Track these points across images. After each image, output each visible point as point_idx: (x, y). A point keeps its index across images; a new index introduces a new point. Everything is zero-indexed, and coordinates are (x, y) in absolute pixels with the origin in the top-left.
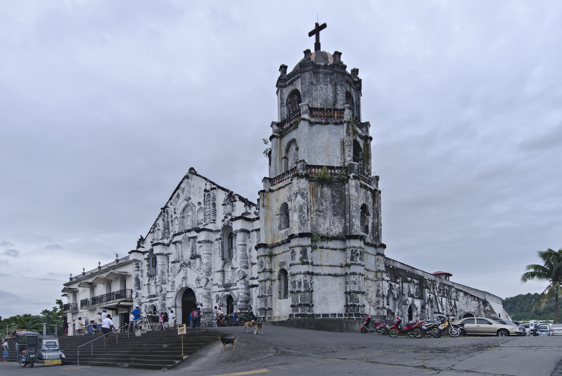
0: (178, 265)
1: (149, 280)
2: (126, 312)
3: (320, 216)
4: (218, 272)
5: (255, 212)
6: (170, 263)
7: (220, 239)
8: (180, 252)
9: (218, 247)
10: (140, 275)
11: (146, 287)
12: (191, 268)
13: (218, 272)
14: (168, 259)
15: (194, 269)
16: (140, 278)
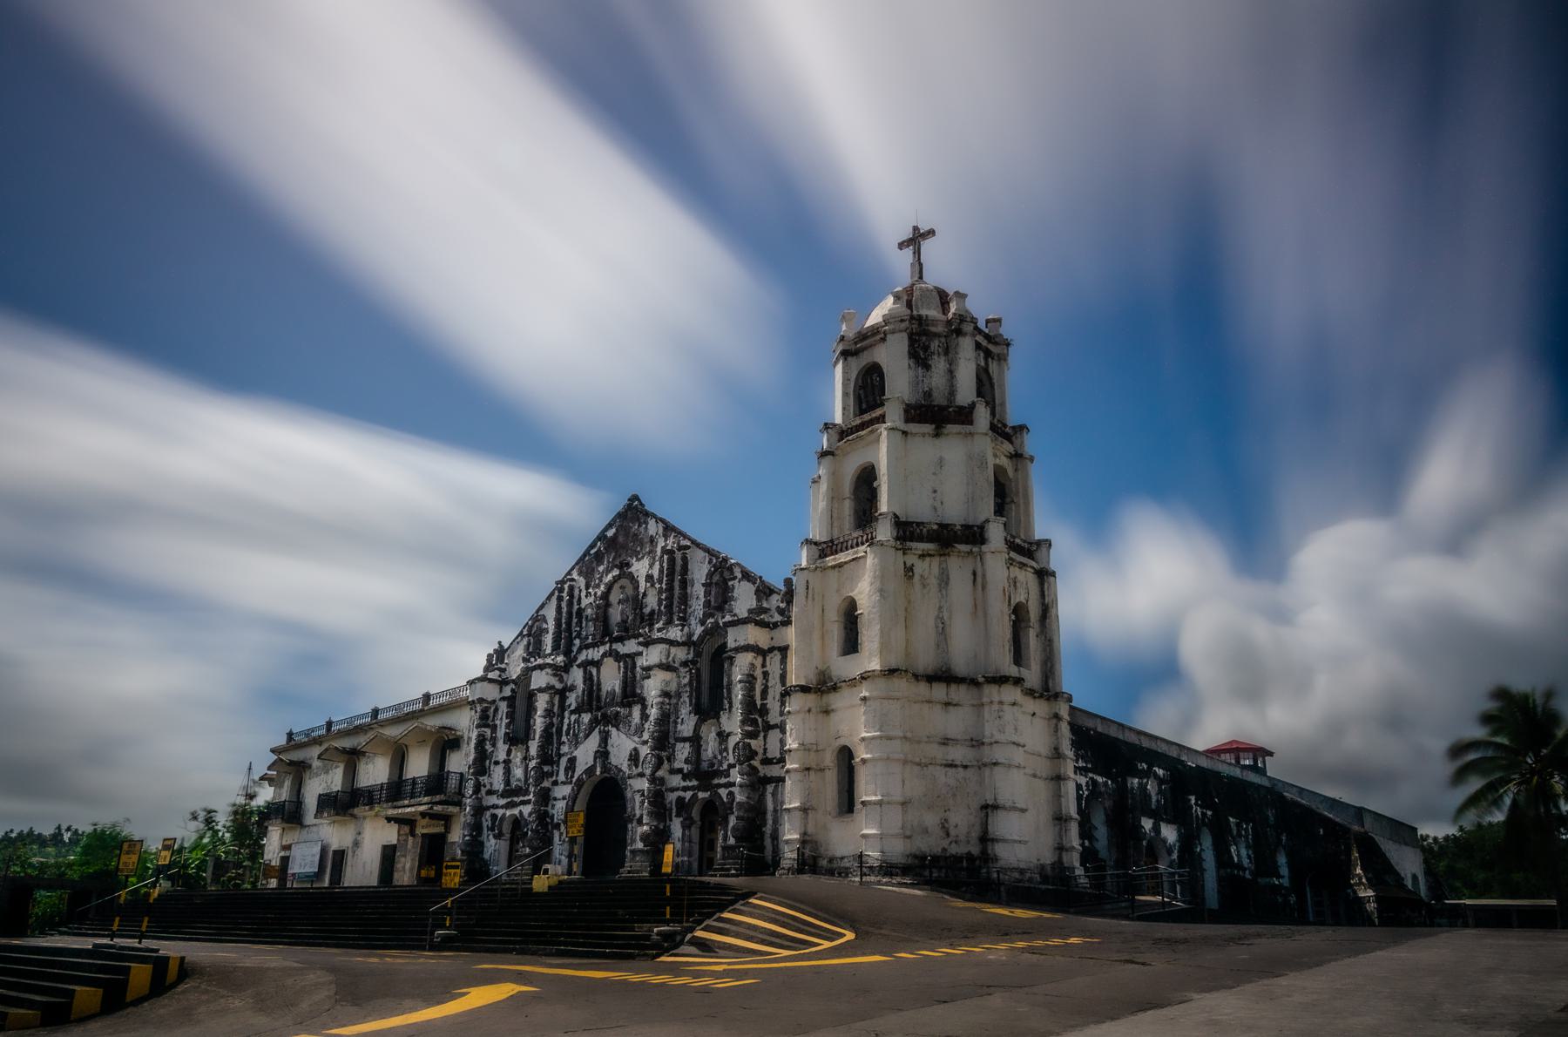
1: (509, 752)
2: (441, 830)
16: (488, 747)
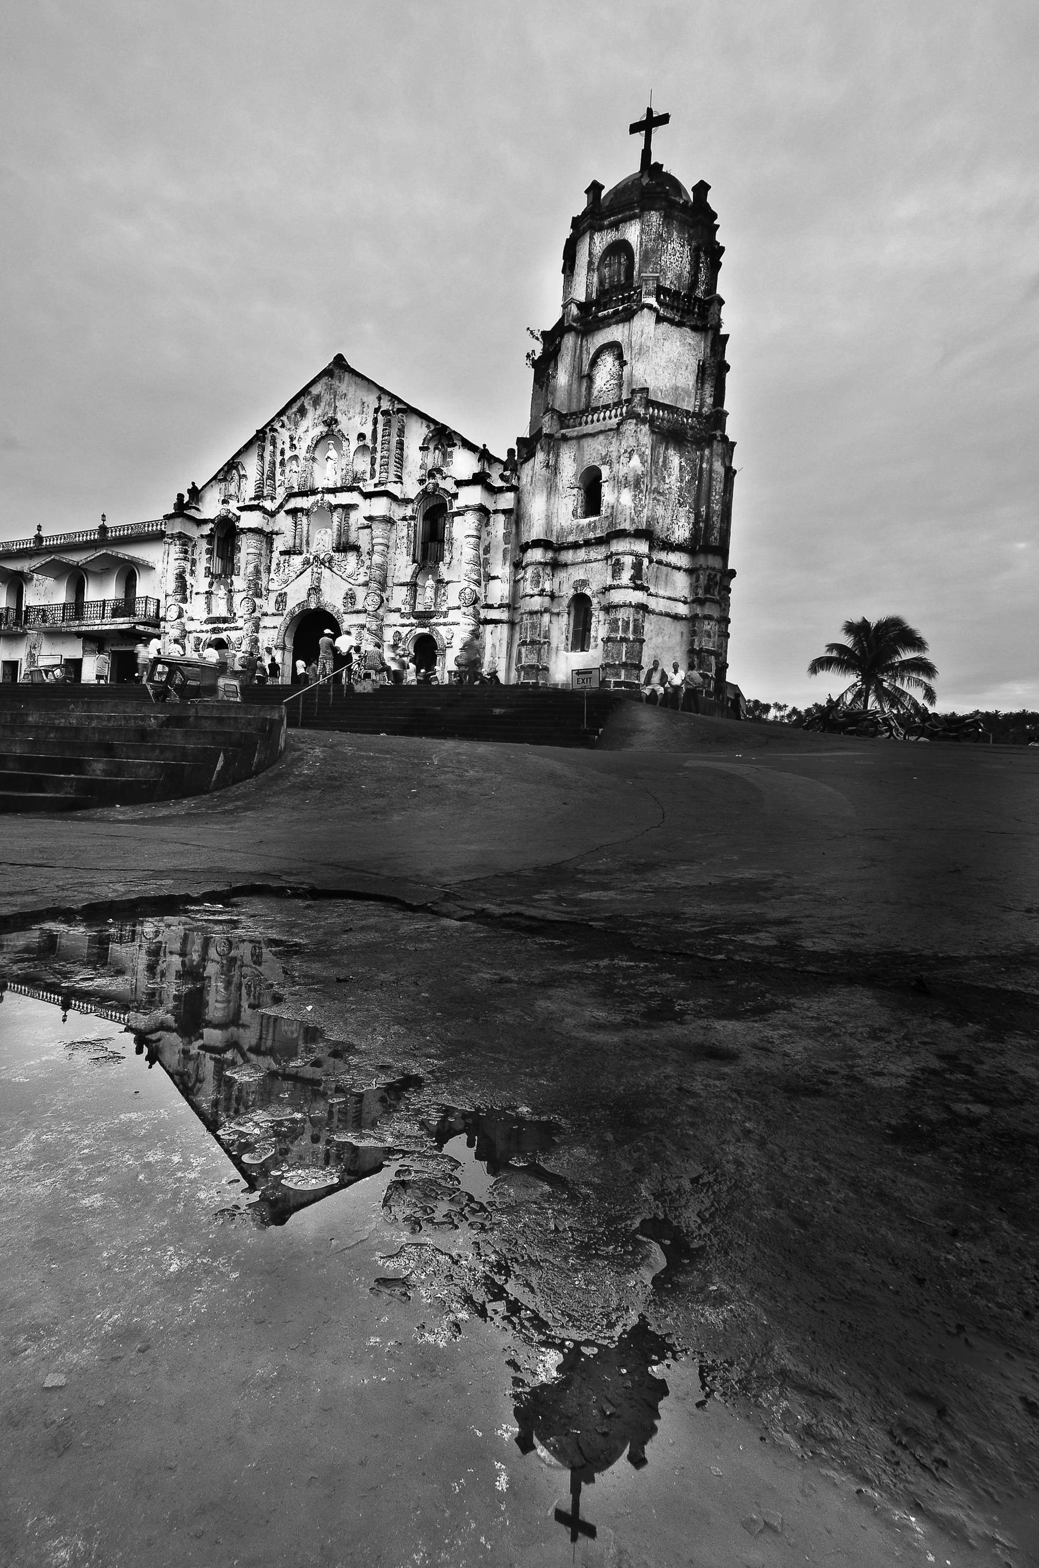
0: (297, 561)
1: (211, 585)
3: (658, 501)
4: (402, 585)
5: (502, 474)
6: (276, 554)
7: (413, 518)
8: (305, 532)
9: (405, 533)
10: (188, 570)
11: (202, 599)
12: (334, 569)
13: (402, 585)
14: (272, 544)
15: (340, 573)
16: (188, 577)
